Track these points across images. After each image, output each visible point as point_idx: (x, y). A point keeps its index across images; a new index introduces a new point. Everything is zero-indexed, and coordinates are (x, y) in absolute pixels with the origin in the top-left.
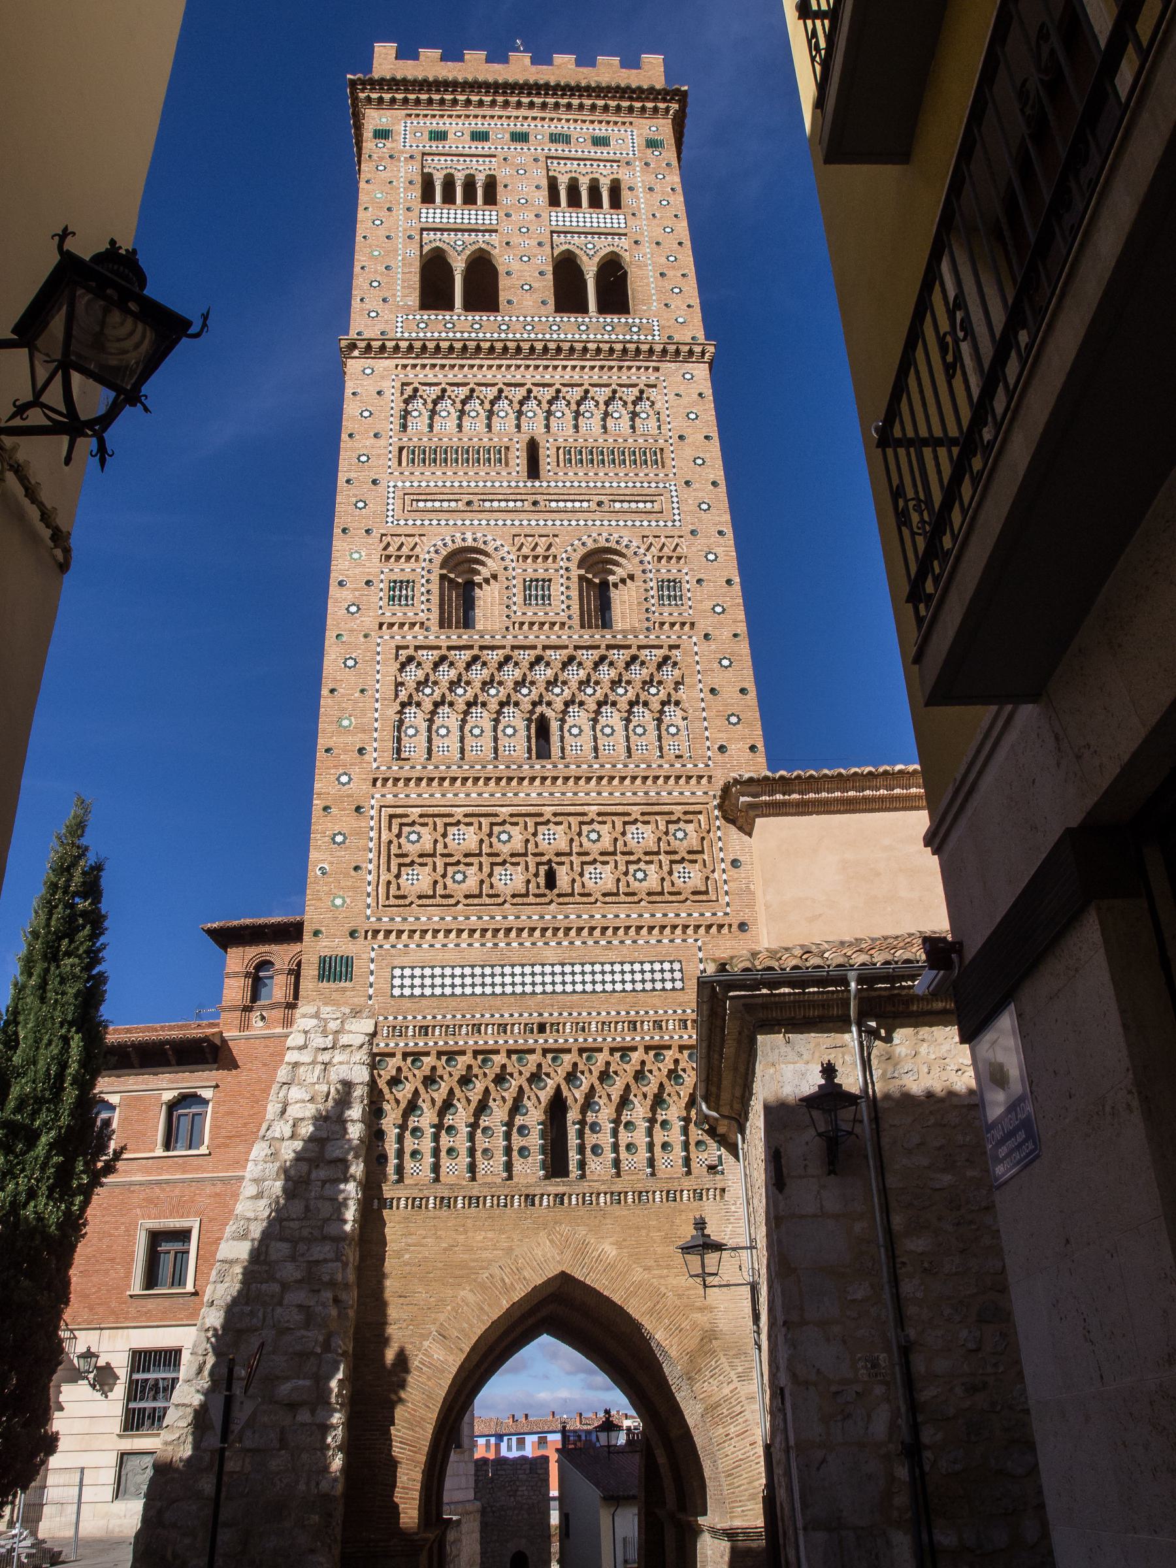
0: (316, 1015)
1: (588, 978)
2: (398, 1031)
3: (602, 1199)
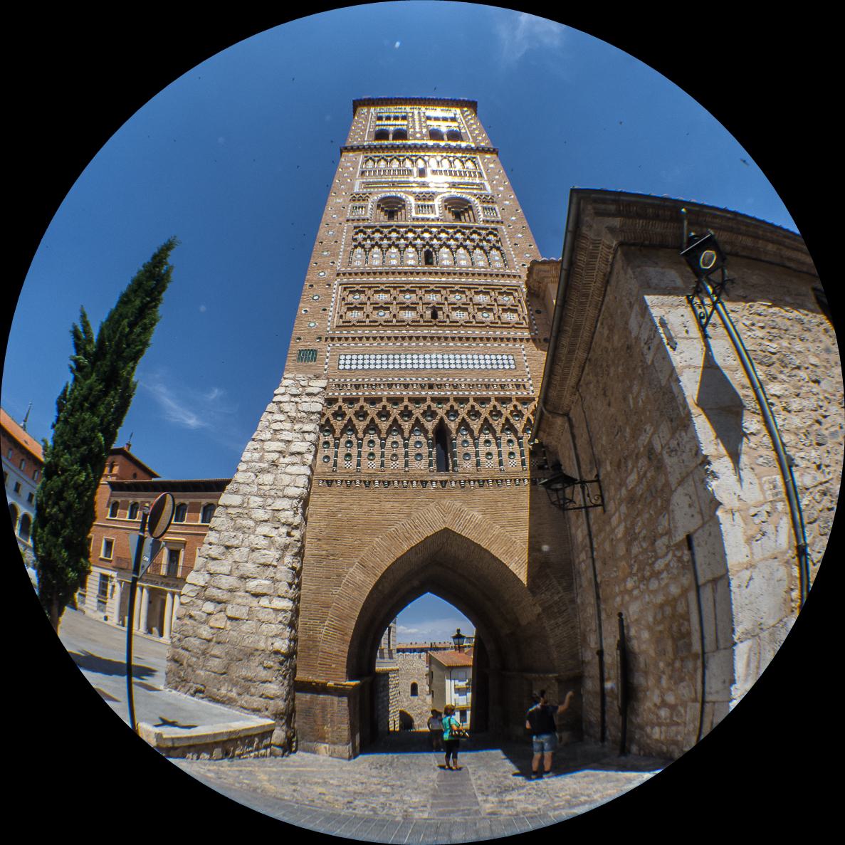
0: (294, 379)
1: (458, 361)
2: (340, 386)
3: (472, 483)
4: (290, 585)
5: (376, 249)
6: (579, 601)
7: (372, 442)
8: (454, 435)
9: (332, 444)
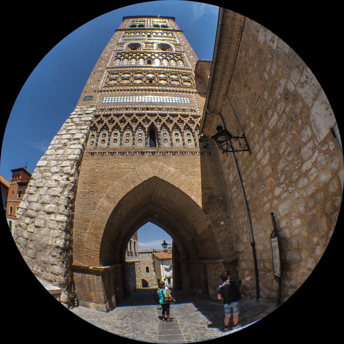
2: (102, 110)
3: (169, 153)
4: (66, 207)
5: (126, 59)
6: (232, 216)
7: (116, 134)
8: (159, 130)
9: (95, 136)
